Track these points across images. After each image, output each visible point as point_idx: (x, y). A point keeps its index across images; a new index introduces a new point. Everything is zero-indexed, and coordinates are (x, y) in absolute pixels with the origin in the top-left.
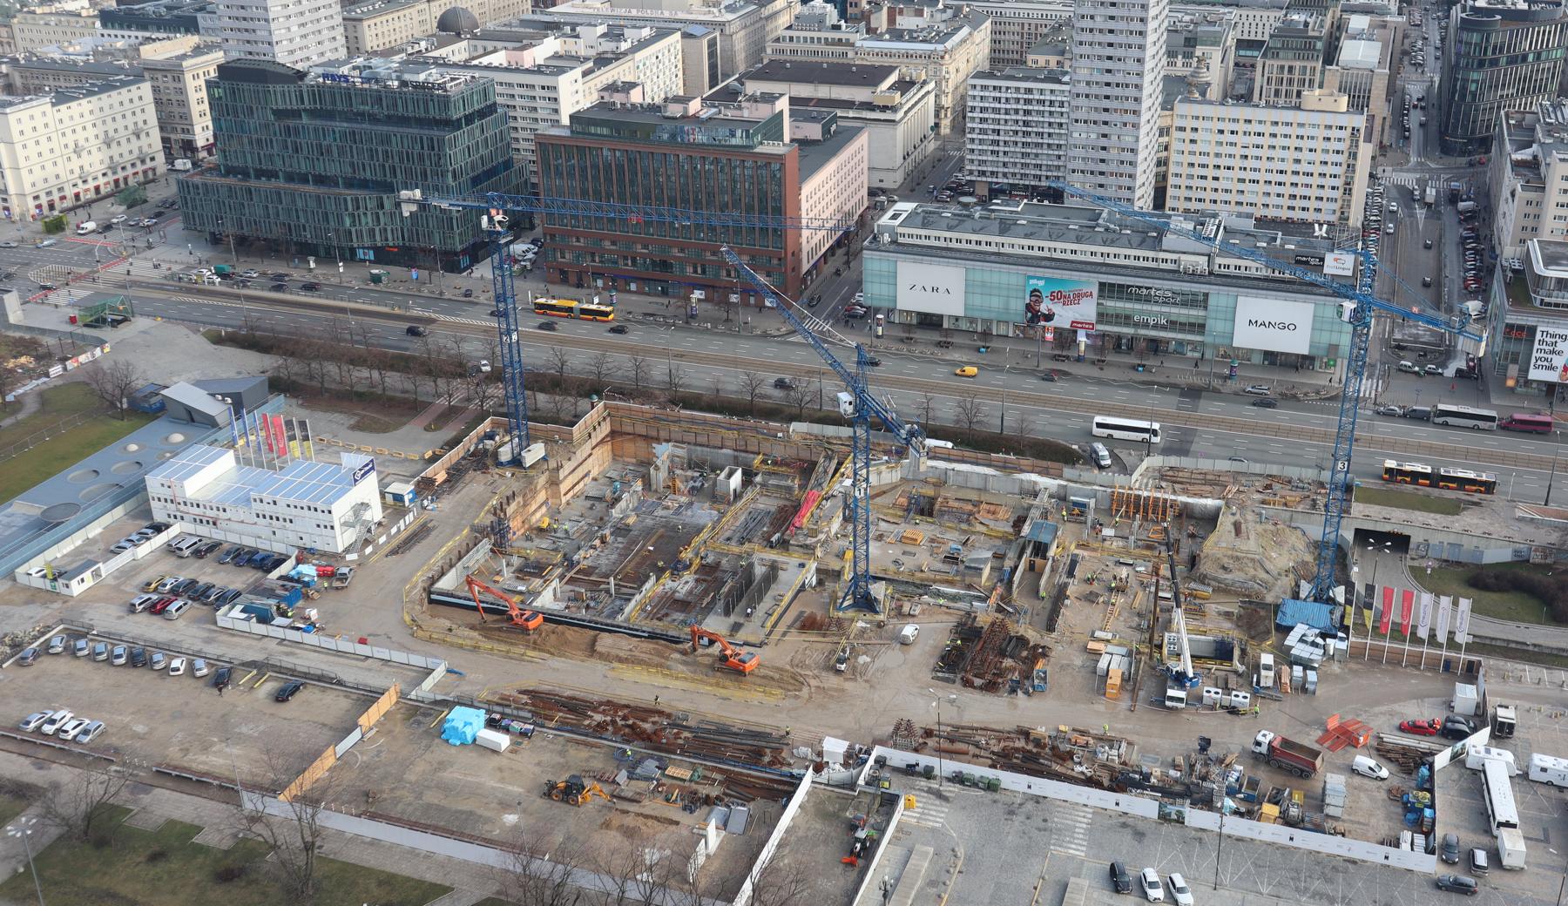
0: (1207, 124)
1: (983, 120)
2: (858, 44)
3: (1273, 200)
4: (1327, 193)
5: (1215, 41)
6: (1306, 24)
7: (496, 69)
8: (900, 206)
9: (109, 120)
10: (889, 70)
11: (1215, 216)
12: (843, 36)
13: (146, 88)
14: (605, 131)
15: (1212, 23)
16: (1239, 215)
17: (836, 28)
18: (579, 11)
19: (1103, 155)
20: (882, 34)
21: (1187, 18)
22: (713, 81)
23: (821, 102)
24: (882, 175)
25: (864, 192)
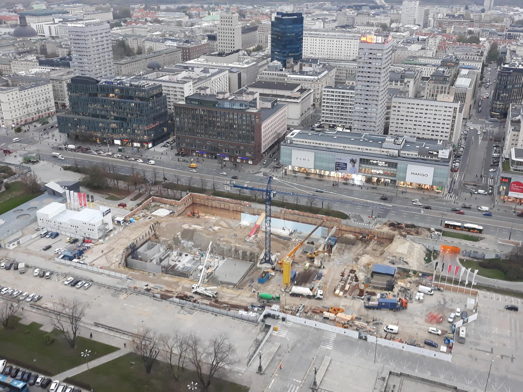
0: (404, 105)
1: (328, 103)
2: (289, 76)
5: (410, 77)
6: (444, 72)
7: (164, 81)
8: (295, 131)
9: (37, 96)
10: (298, 85)
12: (284, 73)
13: (50, 86)
17: (282, 70)
18: (196, 63)
19: (365, 115)
20: (297, 73)
21: (403, 69)
22: (240, 87)
23: (274, 96)
24: (293, 121)
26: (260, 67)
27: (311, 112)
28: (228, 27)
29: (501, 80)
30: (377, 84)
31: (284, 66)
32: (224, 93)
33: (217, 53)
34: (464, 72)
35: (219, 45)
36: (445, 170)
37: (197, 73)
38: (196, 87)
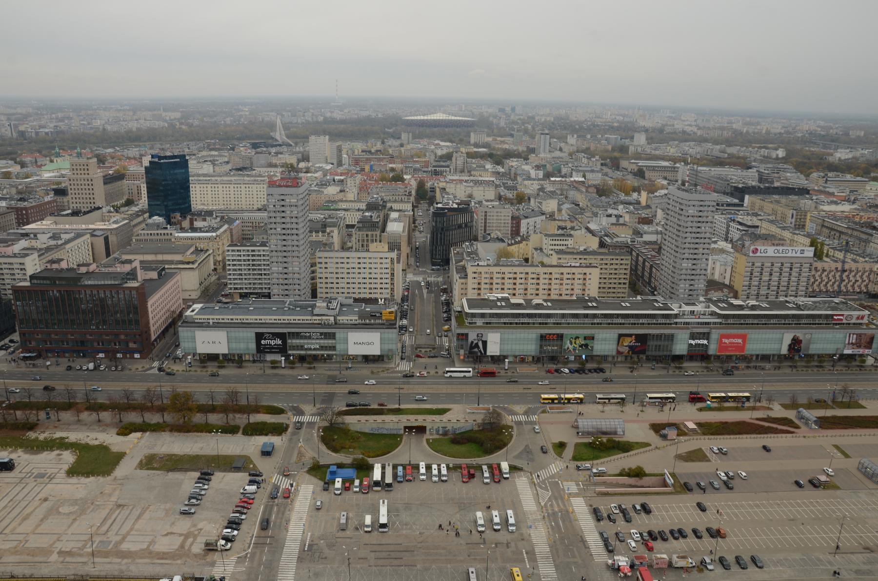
3: (362, 290)
4: (384, 286)
5: (334, 225)
6: (371, 217)
10: (192, 245)
11: (336, 299)
12: (169, 232)
14: (48, 282)
15: (333, 218)
16: (346, 298)
17: (166, 228)
19: (286, 276)
24: (189, 293)
25: (181, 301)
26: (134, 226)
27: (213, 278)
28: (83, 176)
29: (436, 222)
30: (295, 237)
31: (169, 222)
32: (88, 265)
33: (69, 211)
34: (394, 215)
35: (71, 201)
36: (393, 334)
37: (43, 241)
38: (44, 261)
